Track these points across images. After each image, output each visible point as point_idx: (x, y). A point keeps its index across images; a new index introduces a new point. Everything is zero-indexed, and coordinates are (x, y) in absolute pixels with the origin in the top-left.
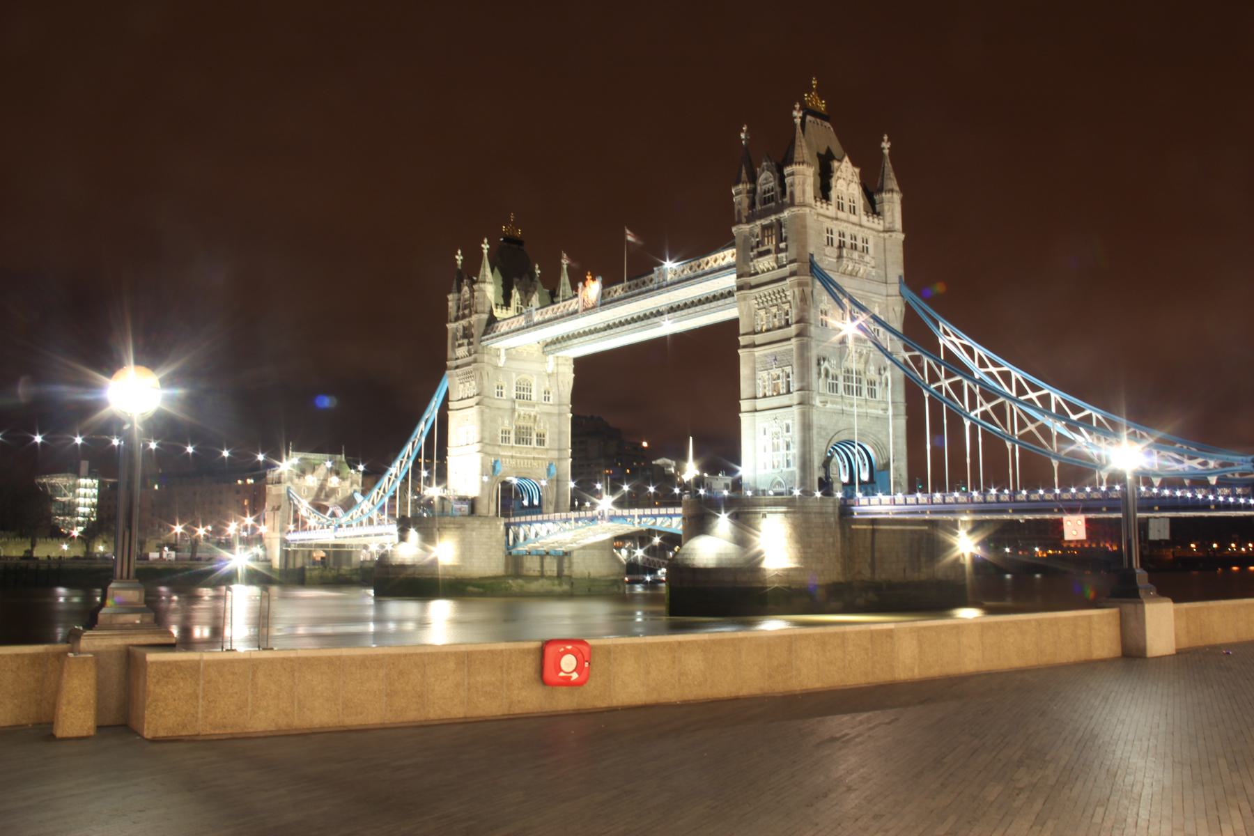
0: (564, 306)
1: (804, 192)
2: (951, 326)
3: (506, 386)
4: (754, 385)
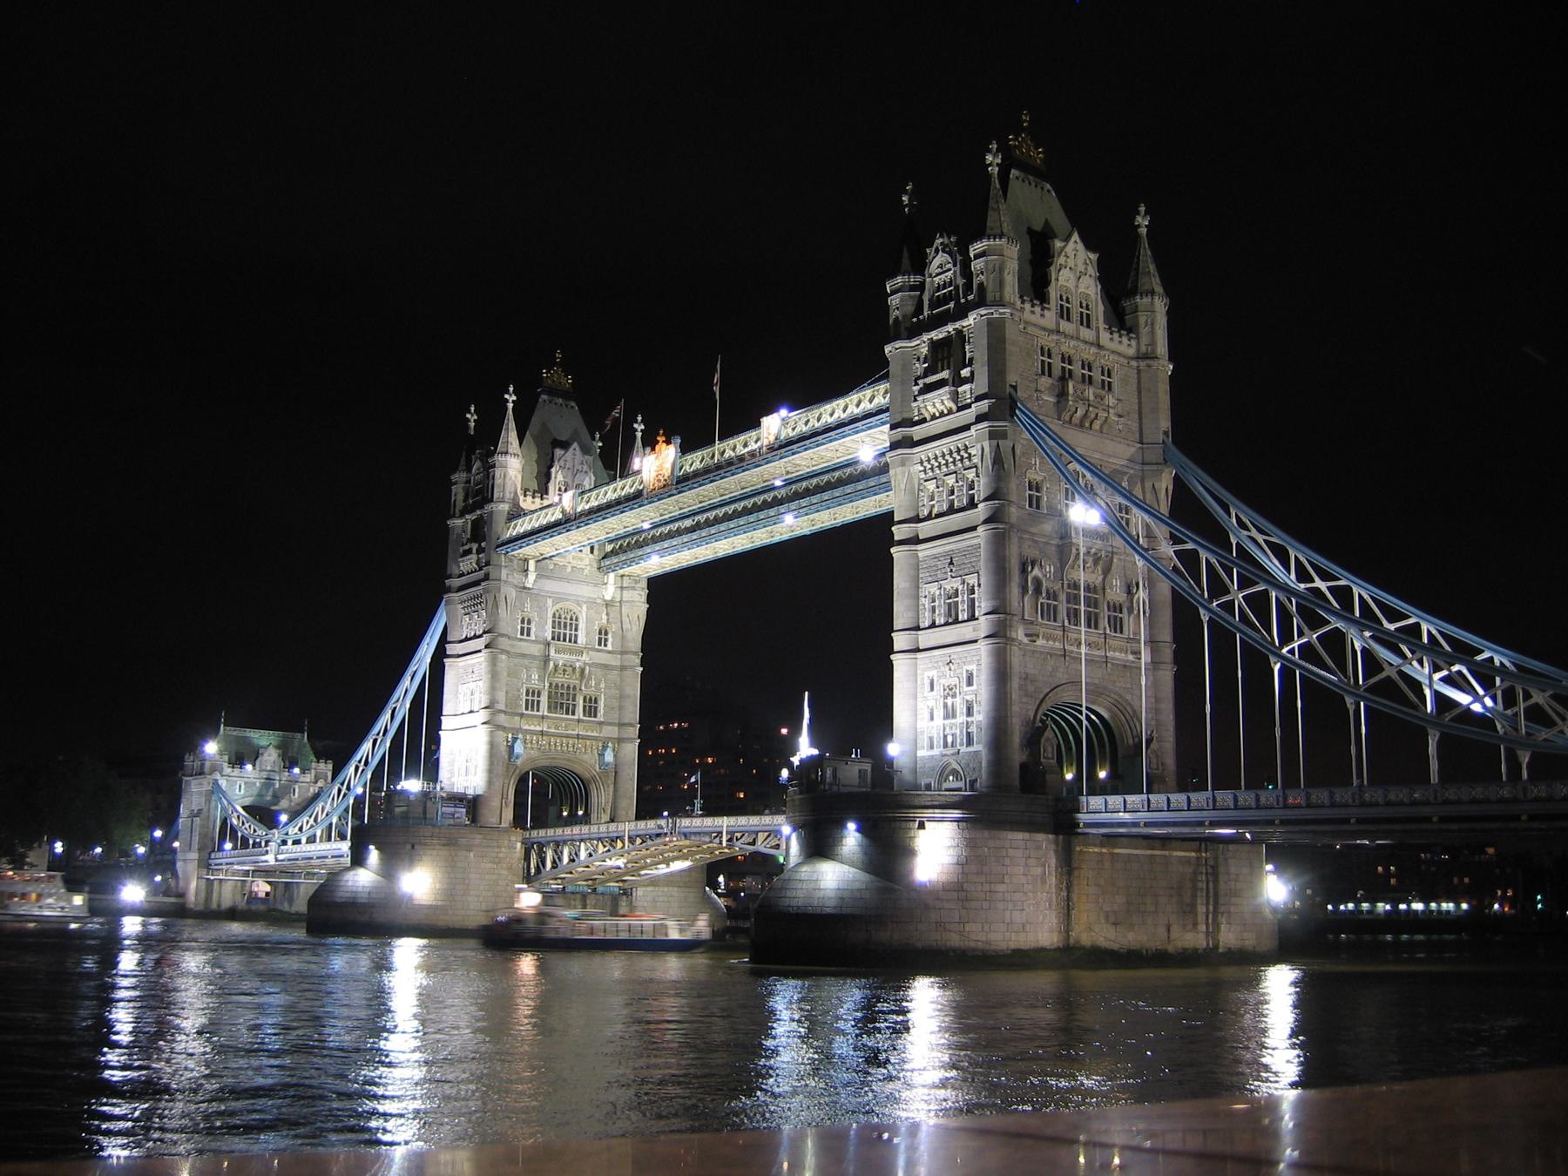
0: (623, 489)
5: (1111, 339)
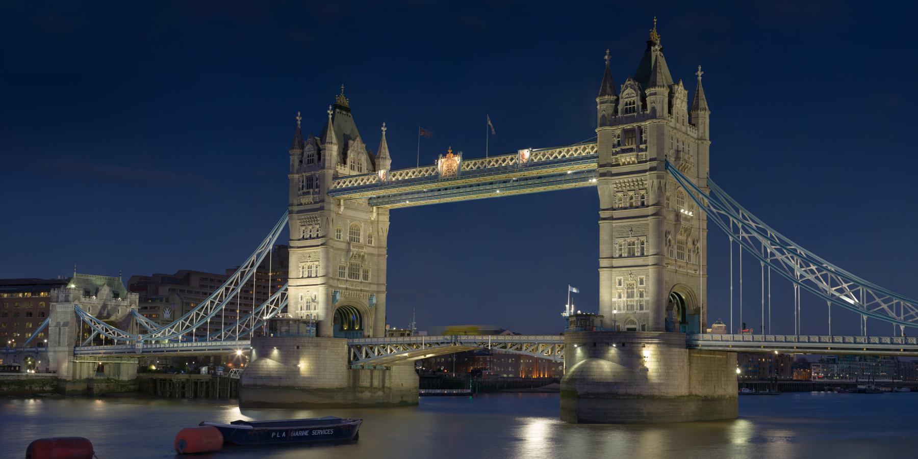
1: (663, 108)
3: (343, 230)
5: (690, 131)
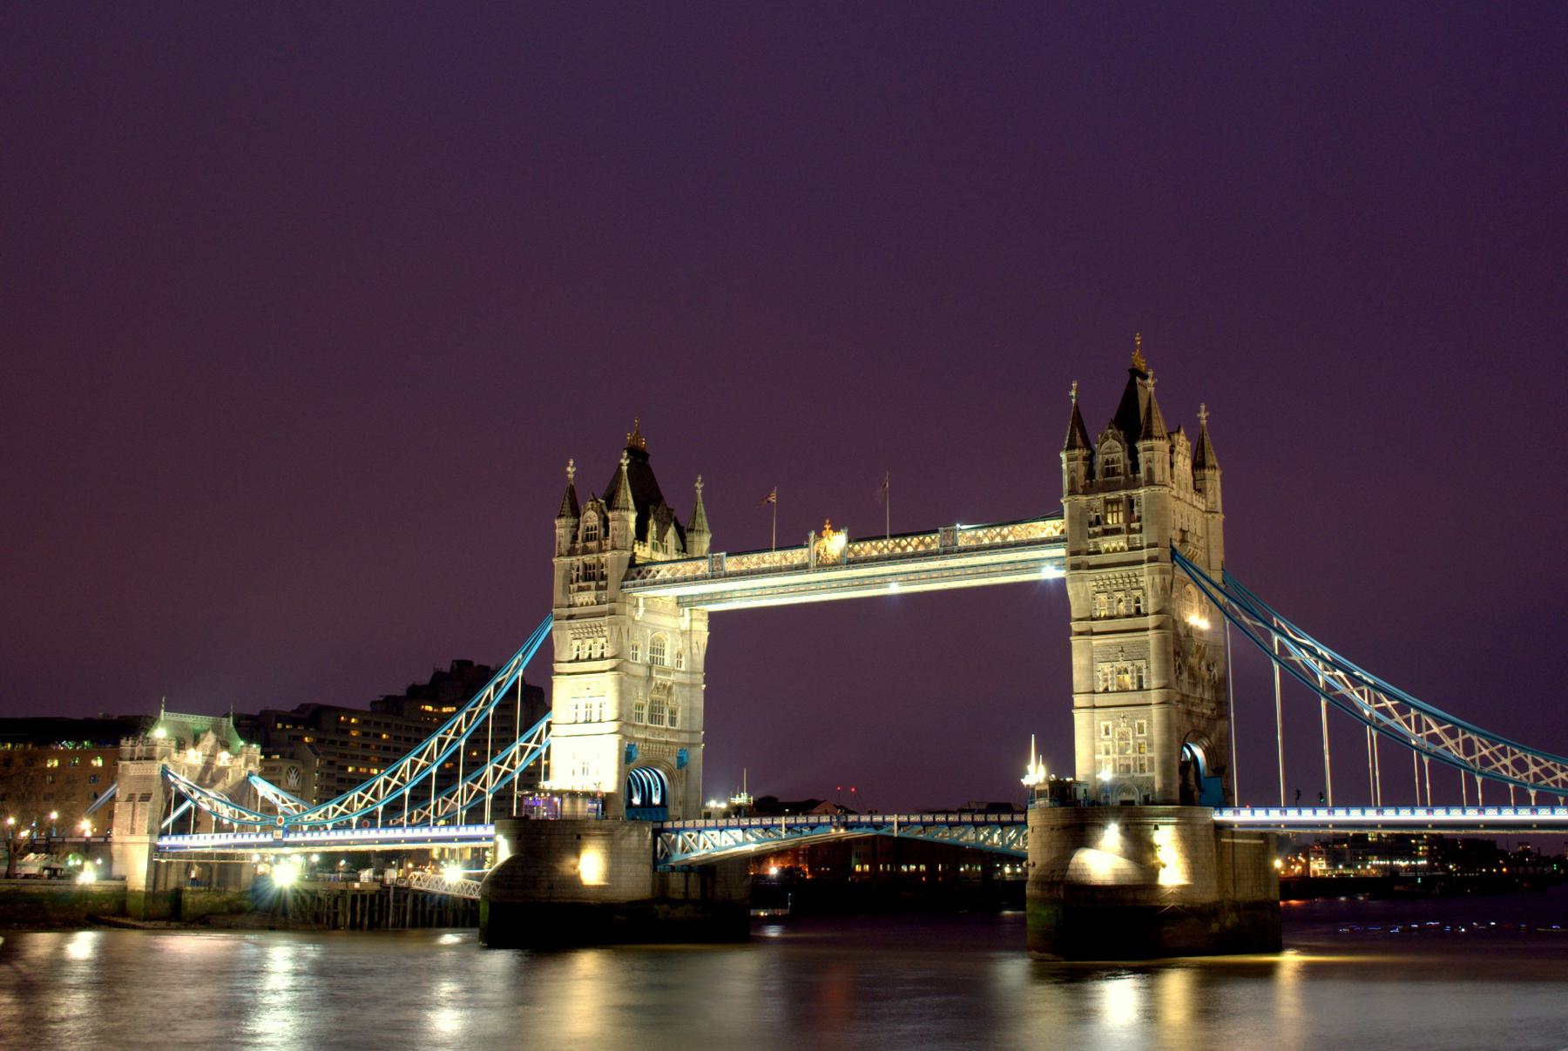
2: (1290, 623)
3: (641, 645)
4: (1092, 678)
